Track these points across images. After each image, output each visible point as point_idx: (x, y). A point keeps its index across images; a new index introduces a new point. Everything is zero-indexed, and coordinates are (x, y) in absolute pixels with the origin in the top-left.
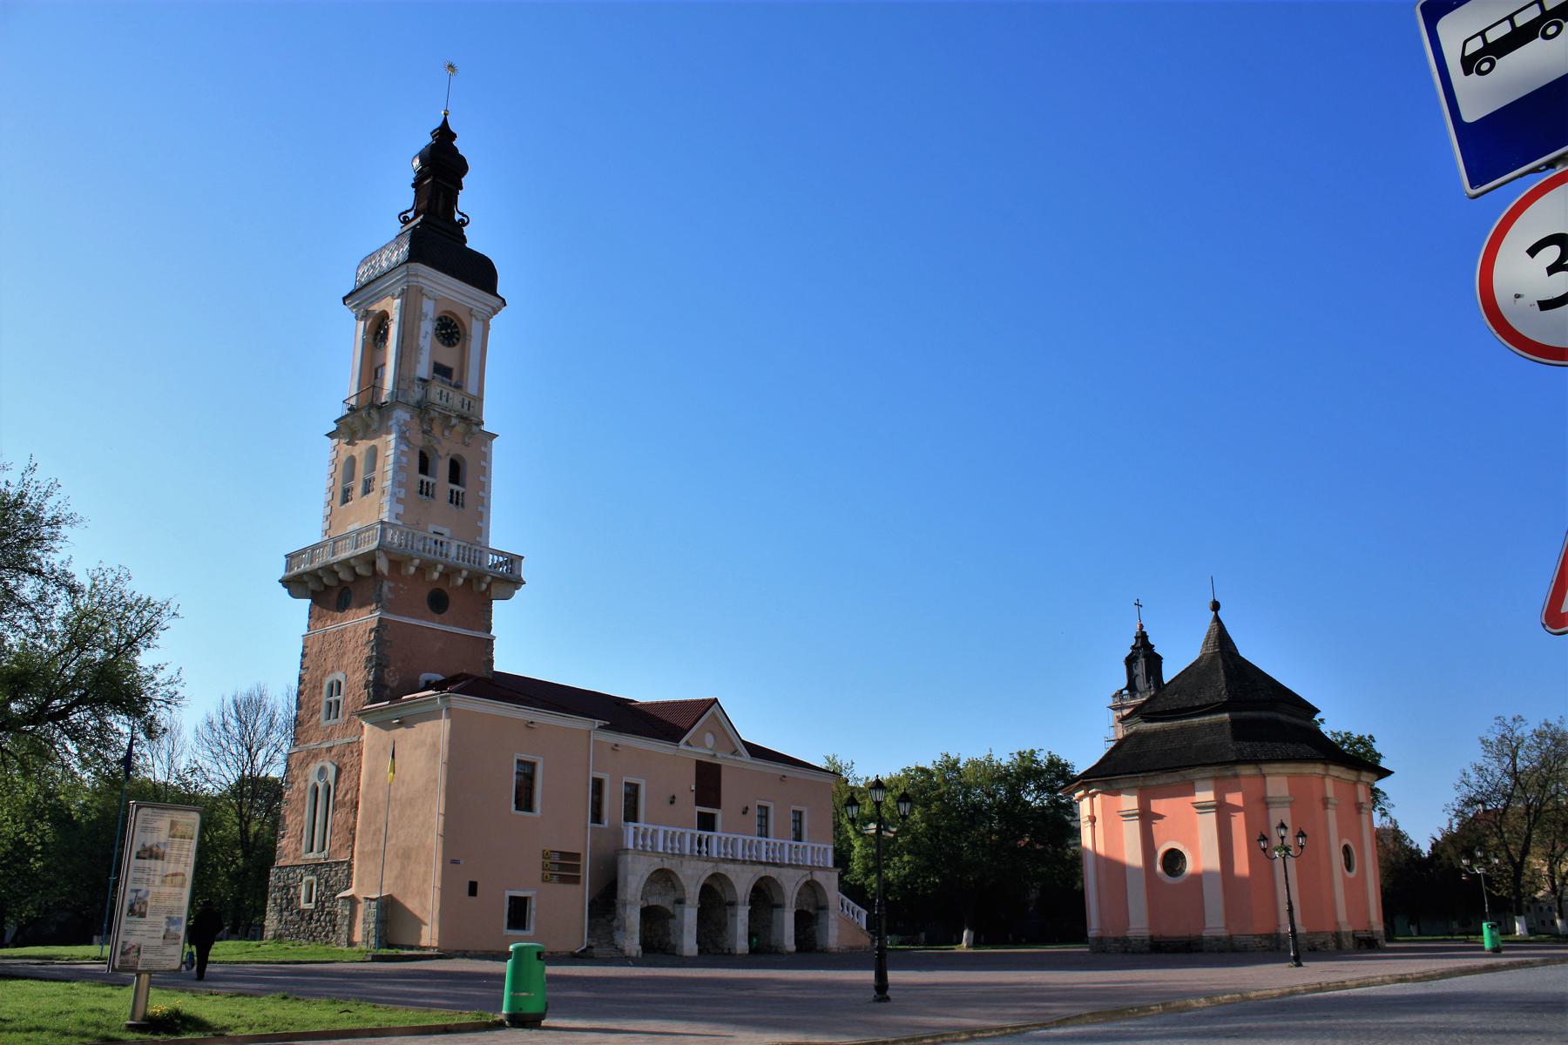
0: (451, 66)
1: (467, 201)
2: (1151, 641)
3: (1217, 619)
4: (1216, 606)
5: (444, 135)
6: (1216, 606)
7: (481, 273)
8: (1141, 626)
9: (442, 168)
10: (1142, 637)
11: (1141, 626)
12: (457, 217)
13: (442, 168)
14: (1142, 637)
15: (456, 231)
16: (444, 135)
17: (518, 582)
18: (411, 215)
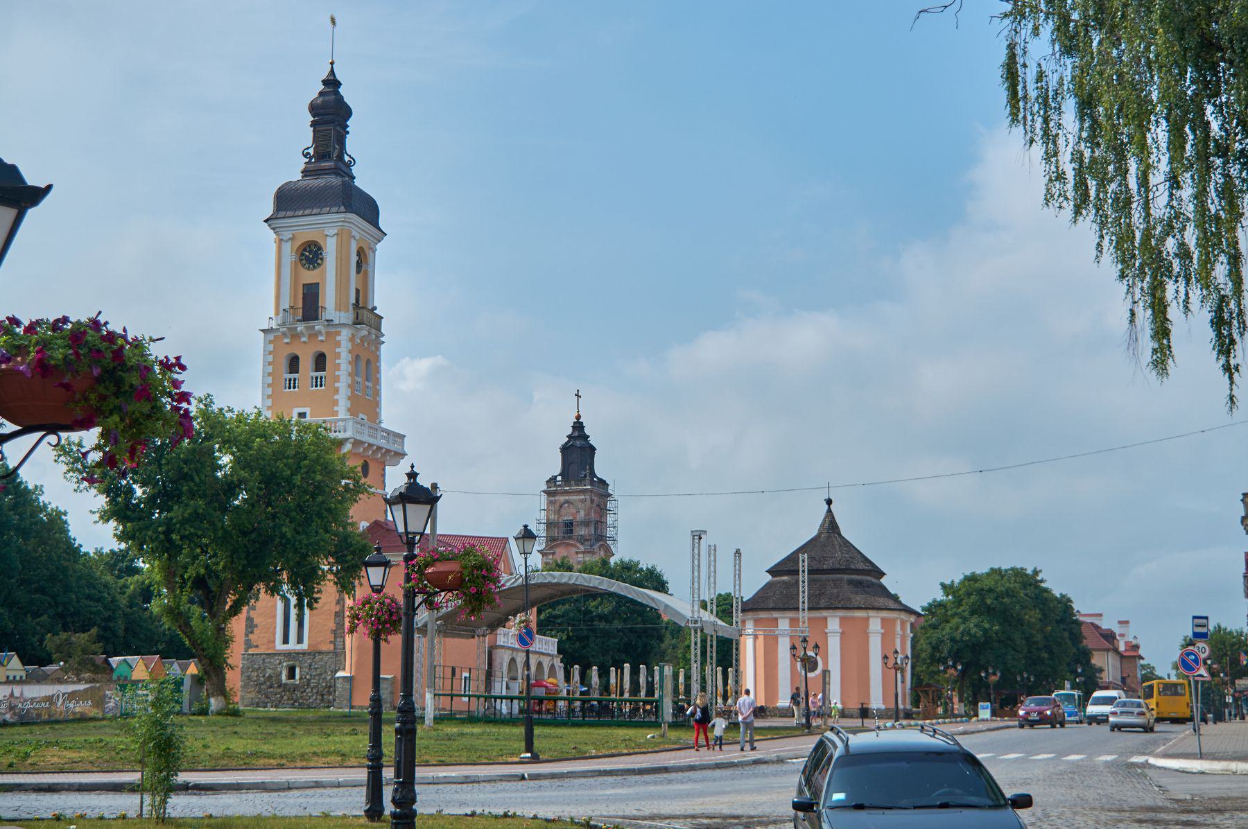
0: (333, 21)
1: (353, 145)
2: (587, 431)
3: (829, 511)
4: (829, 502)
5: (332, 83)
6: (829, 502)
7: (368, 210)
8: (578, 417)
9: (331, 113)
10: (578, 426)
11: (578, 417)
12: (347, 158)
13: (331, 113)
14: (578, 426)
15: (344, 169)
16: (332, 83)
17: (403, 455)
18: (311, 151)
